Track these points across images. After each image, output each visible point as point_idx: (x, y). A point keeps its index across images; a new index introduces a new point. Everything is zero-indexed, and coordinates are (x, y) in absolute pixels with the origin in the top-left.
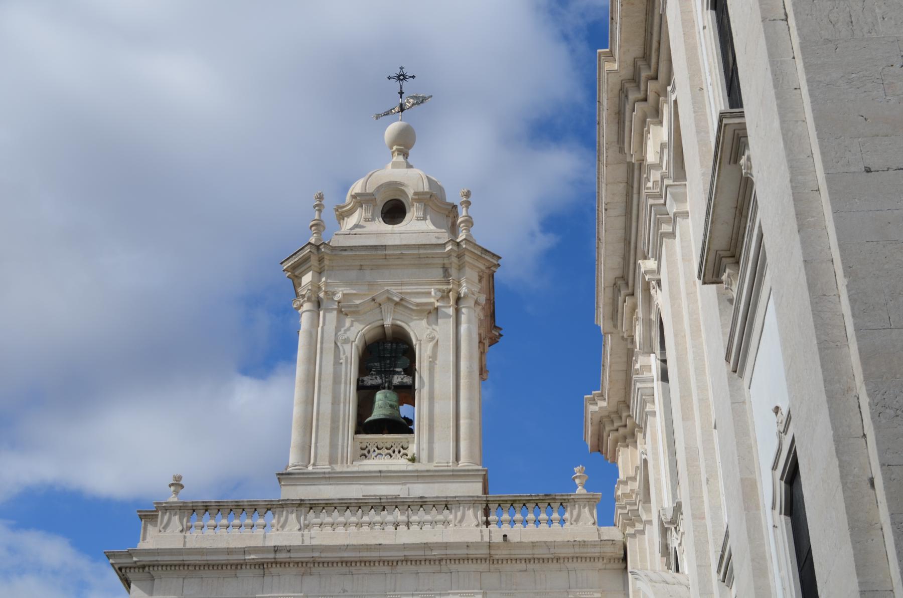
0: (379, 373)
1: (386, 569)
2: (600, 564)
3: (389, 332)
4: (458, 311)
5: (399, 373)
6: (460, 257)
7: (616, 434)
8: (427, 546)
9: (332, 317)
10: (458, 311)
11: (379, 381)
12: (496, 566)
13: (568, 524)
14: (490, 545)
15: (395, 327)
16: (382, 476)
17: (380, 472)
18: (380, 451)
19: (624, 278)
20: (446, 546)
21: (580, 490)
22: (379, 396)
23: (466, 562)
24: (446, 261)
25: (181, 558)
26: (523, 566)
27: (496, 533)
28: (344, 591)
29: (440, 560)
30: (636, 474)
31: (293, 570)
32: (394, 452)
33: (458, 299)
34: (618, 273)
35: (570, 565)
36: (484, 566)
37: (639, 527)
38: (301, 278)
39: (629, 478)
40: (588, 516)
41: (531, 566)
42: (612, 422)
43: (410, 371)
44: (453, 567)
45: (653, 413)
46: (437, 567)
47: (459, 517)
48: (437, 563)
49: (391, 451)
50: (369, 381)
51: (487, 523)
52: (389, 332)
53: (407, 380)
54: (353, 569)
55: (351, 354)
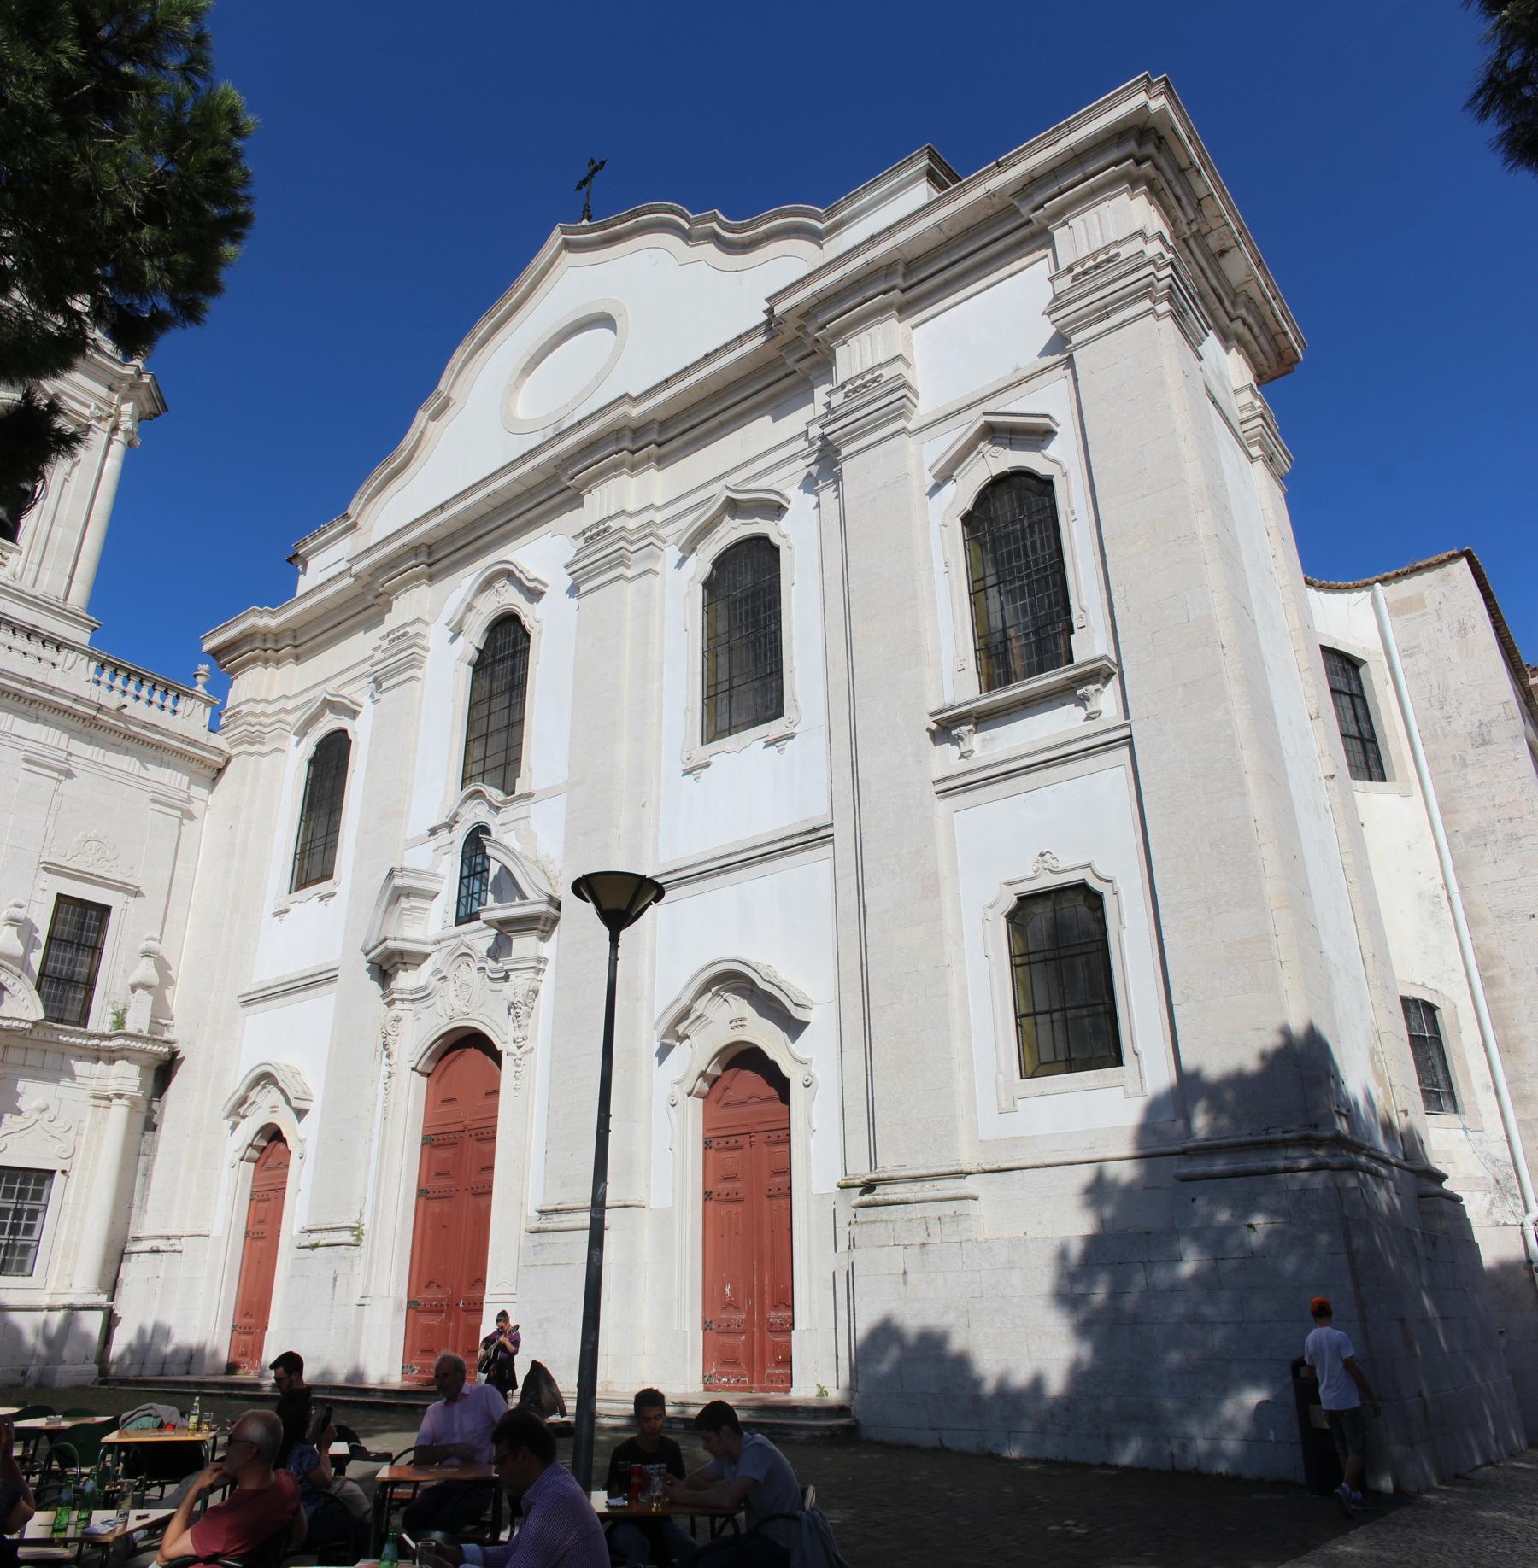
2: (194, 767)
4: (110, 441)
6: (132, 386)
8: (29, 682)
10: (110, 441)
12: (91, 730)
13: (179, 716)
14: (100, 708)
19: (430, 549)
20: (52, 690)
21: (199, 688)
24: (116, 383)
26: (118, 740)
27: (112, 700)
33: (115, 429)
34: (429, 541)
35: (166, 757)
36: (79, 725)
40: (203, 715)
41: (126, 743)
42: (265, 641)
44: (44, 713)
46: (24, 707)
47: (68, 665)
51: (98, 683)
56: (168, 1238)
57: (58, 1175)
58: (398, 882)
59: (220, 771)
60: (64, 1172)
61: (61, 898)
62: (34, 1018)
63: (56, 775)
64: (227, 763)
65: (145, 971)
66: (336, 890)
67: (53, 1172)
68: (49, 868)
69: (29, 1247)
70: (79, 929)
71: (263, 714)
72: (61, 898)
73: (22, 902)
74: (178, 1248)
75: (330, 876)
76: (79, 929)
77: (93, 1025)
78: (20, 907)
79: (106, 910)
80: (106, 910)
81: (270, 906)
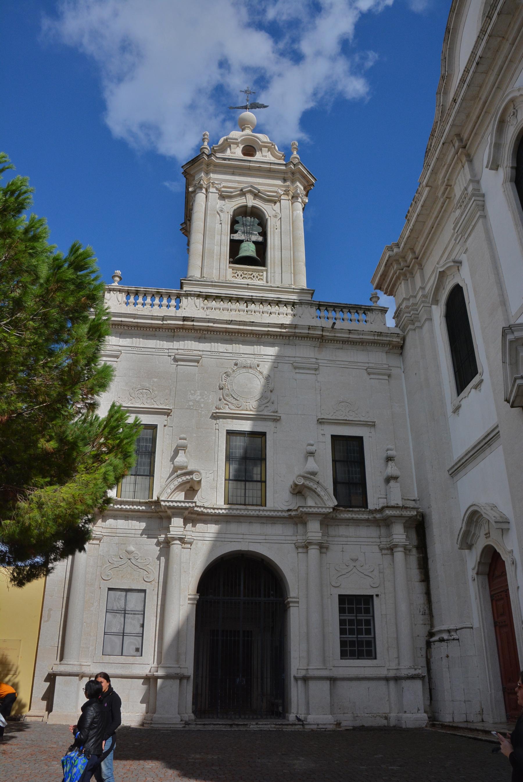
0: (244, 233)
1: (254, 339)
3: (249, 210)
5: (256, 235)
7: (401, 271)
9: (214, 196)
11: (242, 237)
14: (323, 329)
15: (253, 207)
16: (248, 287)
17: (248, 285)
18: (246, 276)
22: (244, 245)
23: (306, 339)
25: (120, 319)
28: (227, 350)
29: (289, 337)
30: (417, 293)
31: (193, 334)
32: (254, 277)
37: (417, 324)
38: (194, 177)
39: (412, 296)
43: (264, 234)
45: (484, 216)
48: (287, 338)
49: (252, 276)
50: (236, 237)
52: (249, 210)
53: (260, 239)
54: (233, 337)
55: (227, 219)
56: (449, 631)
57: (375, 597)
58: (510, 337)
59: (402, 347)
60: (377, 595)
61: (333, 436)
62: (332, 505)
63: (313, 372)
64: (404, 339)
65: (392, 469)
66: (483, 378)
67: (372, 596)
68: (321, 422)
69: (370, 642)
70: (349, 453)
71: (413, 304)
72: (333, 436)
73: (312, 442)
74: (456, 637)
75: (477, 373)
76: (349, 453)
77: (371, 506)
78: (312, 445)
79: (360, 439)
80: (360, 439)
81: (450, 409)
